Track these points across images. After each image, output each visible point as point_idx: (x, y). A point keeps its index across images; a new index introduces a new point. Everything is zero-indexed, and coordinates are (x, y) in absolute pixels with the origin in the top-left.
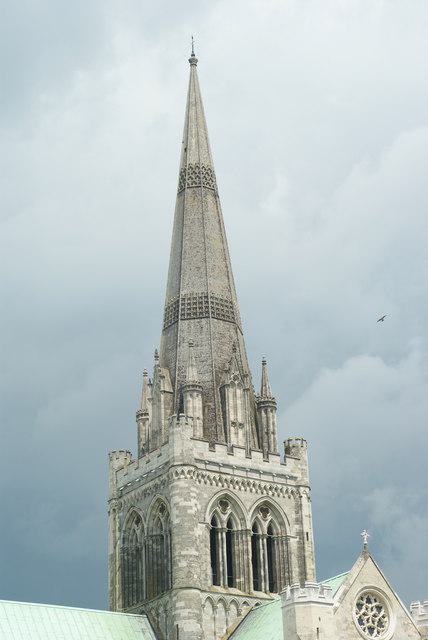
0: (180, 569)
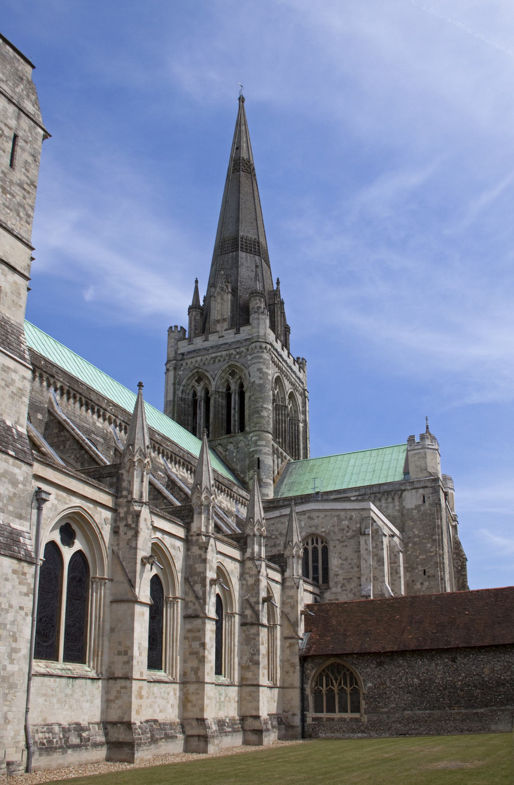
0: (263, 417)
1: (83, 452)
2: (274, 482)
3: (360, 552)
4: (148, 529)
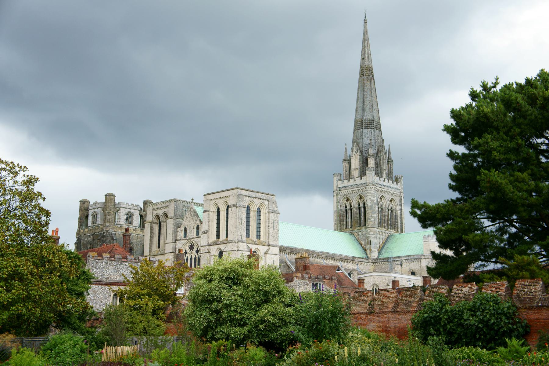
2: (378, 250)
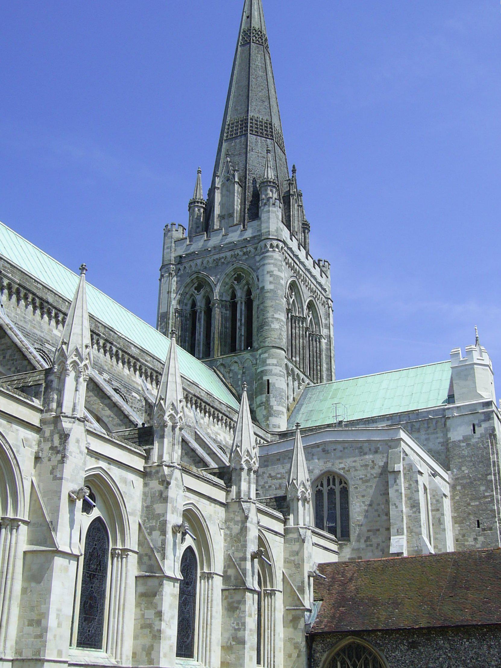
0: (274, 330)
1: (26, 363)
3: (388, 494)
4: (81, 452)
